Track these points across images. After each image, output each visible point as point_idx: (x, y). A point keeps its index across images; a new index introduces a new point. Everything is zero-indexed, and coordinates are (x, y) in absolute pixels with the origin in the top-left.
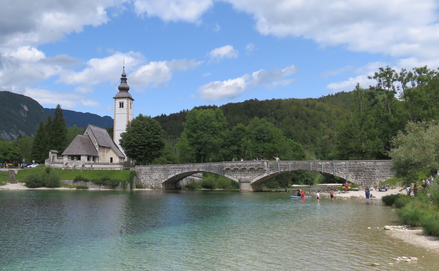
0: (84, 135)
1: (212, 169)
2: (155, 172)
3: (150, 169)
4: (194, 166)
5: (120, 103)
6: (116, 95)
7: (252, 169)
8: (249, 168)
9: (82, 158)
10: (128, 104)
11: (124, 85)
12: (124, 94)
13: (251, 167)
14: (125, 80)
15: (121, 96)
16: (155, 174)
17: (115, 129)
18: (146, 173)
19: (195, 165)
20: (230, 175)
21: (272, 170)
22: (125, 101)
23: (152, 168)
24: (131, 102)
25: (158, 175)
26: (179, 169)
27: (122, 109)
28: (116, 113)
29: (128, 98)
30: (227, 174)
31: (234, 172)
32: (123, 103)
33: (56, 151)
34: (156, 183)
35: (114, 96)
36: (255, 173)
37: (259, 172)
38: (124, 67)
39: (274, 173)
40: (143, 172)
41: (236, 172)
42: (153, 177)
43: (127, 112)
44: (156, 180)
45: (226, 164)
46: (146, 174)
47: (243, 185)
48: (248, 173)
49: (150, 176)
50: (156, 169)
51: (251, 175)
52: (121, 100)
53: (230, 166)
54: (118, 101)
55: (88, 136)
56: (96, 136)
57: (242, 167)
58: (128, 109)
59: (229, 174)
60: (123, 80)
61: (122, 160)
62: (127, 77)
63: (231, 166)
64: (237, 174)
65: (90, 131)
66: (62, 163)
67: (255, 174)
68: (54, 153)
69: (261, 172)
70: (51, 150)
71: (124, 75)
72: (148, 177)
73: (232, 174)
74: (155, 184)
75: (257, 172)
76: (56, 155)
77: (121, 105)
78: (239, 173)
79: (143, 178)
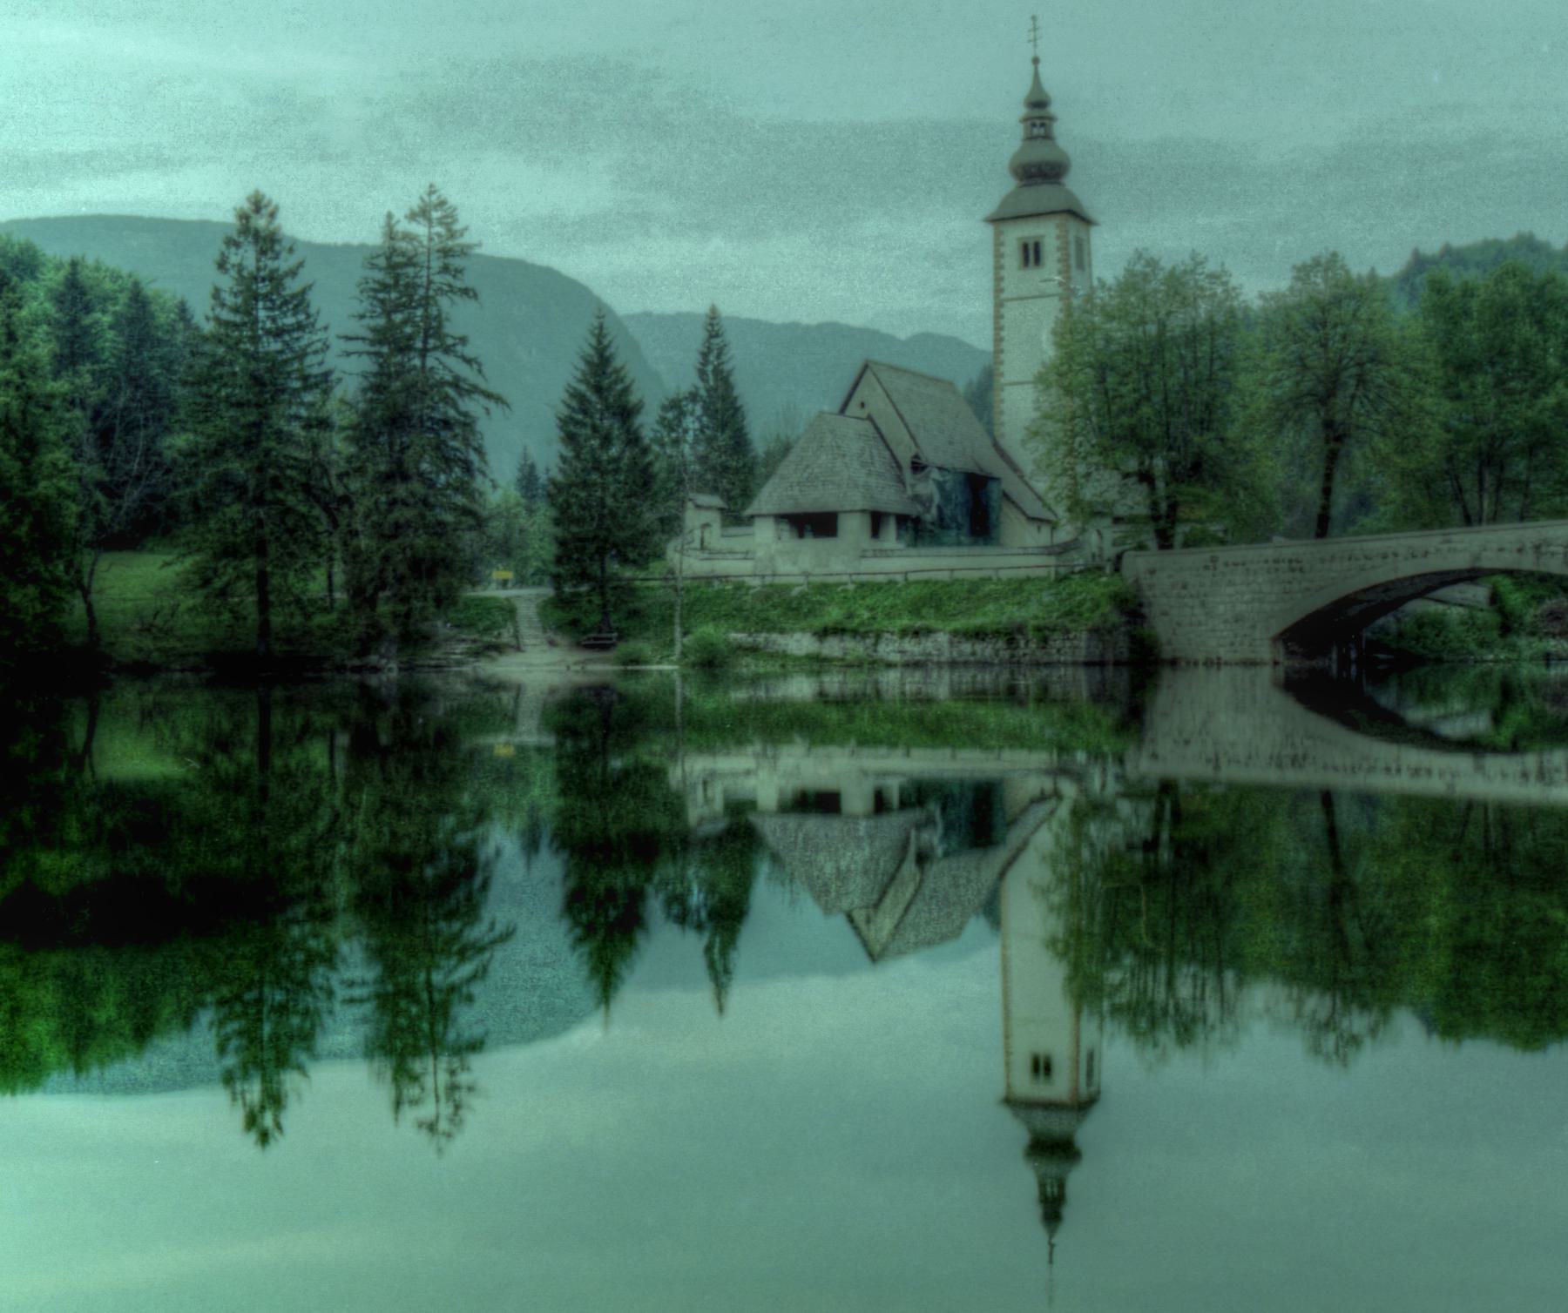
0: (849, 412)
1: (1553, 554)
2: (1231, 583)
3: (1206, 568)
4: (1448, 542)
5: (1025, 247)
6: (1005, 203)
10: (1064, 248)
11: (1040, 153)
12: (1044, 196)
14: (1043, 125)
15: (1029, 209)
16: (1230, 590)
17: (1003, 380)
18: (1185, 587)
19: (1454, 538)
22: (1048, 233)
23: (1214, 560)
25: (1247, 597)
26: (1362, 562)
27: (1034, 275)
28: (1004, 296)
29: (1064, 216)
32: (1037, 246)
33: (716, 501)
34: (1236, 636)
42: (1221, 608)
43: (1059, 290)
44: (1236, 621)
46: (1184, 592)
49: (1203, 604)
50: (1236, 564)
52: (1028, 230)
54: (1016, 234)
55: (870, 418)
56: (907, 417)
58: (1066, 272)
60: (1034, 125)
61: (1046, 530)
65: (880, 391)
66: (747, 555)
68: (709, 508)
70: (691, 495)
72: (1192, 607)
74: (1232, 644)
76: (714, 518)
77: (1032, 254)
79: (1165, 614)
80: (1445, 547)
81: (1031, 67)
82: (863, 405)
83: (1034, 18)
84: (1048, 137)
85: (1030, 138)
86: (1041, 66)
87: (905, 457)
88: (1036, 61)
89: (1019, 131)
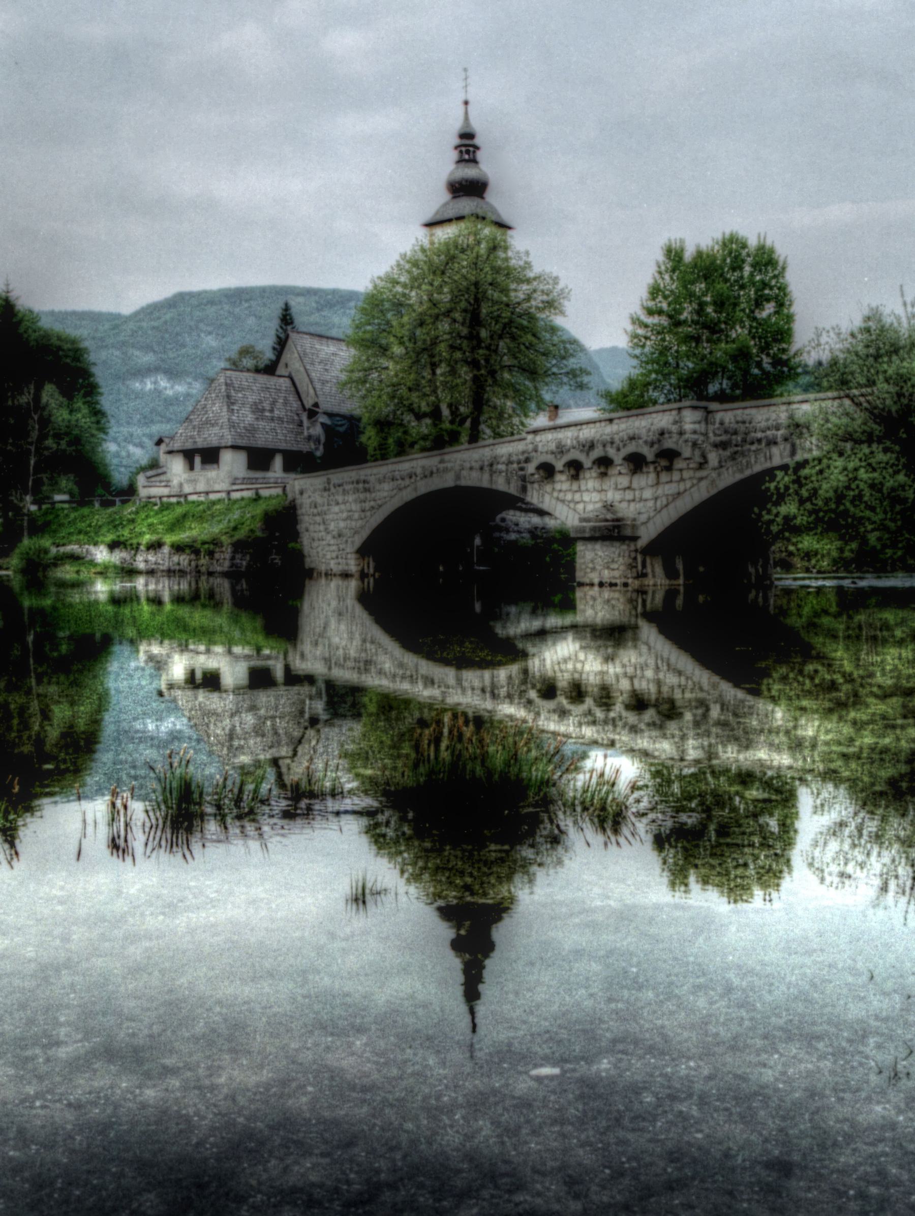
0: (278, 372)
2: (338, 504)
7: (636, 463)
8: (625, 452)
9: (227, 457)
11: (469, 172)
13: (631, 448)
16: (336, 509)
18: (316, 507)
19: (447, 457)
20: (563, 501)
21: (733, 457)
24: (498, 232)
30: (551, 494)
31: (575, 487)
35: (428, 216)
36: (658, 483)
37: (676, 476)
38: (466, 103)
39: (739, 477)
40: (308, 501)
41: (583, 482)
45: (538, 438)
46: (315, 511)
47: (589, 555)
48: (629, 488)
51: (641, 500)
53: (553, 453)
57: (597, 453)
59: (558, 499)
62: (477, 141)
63: (557, 447)
64: (586, 497)
67: (660, 492)
69: (686, 474)
71: (468, 130)
73: (569, 497)
75: (664, 477)
78: (595, 490)
80: (441, 466)
81: (462, 108)
82: (287, 365)
83: (465, 70)
84: (474, 161)
85: (460, 161)
86: (470, 107)
87: (309, 403)
88: (466, 103)
89: (454, 155)
